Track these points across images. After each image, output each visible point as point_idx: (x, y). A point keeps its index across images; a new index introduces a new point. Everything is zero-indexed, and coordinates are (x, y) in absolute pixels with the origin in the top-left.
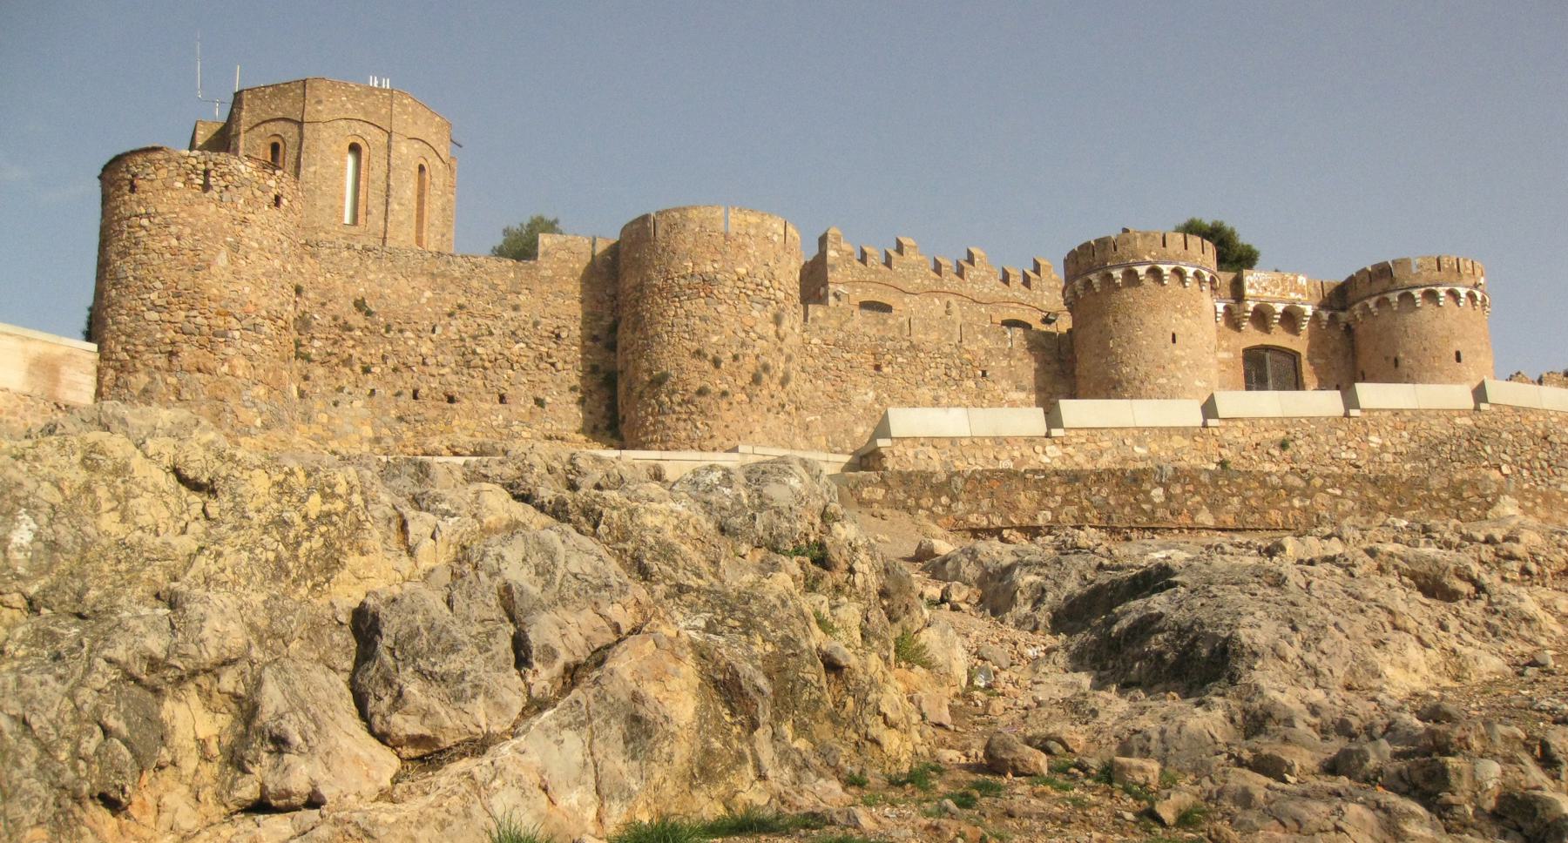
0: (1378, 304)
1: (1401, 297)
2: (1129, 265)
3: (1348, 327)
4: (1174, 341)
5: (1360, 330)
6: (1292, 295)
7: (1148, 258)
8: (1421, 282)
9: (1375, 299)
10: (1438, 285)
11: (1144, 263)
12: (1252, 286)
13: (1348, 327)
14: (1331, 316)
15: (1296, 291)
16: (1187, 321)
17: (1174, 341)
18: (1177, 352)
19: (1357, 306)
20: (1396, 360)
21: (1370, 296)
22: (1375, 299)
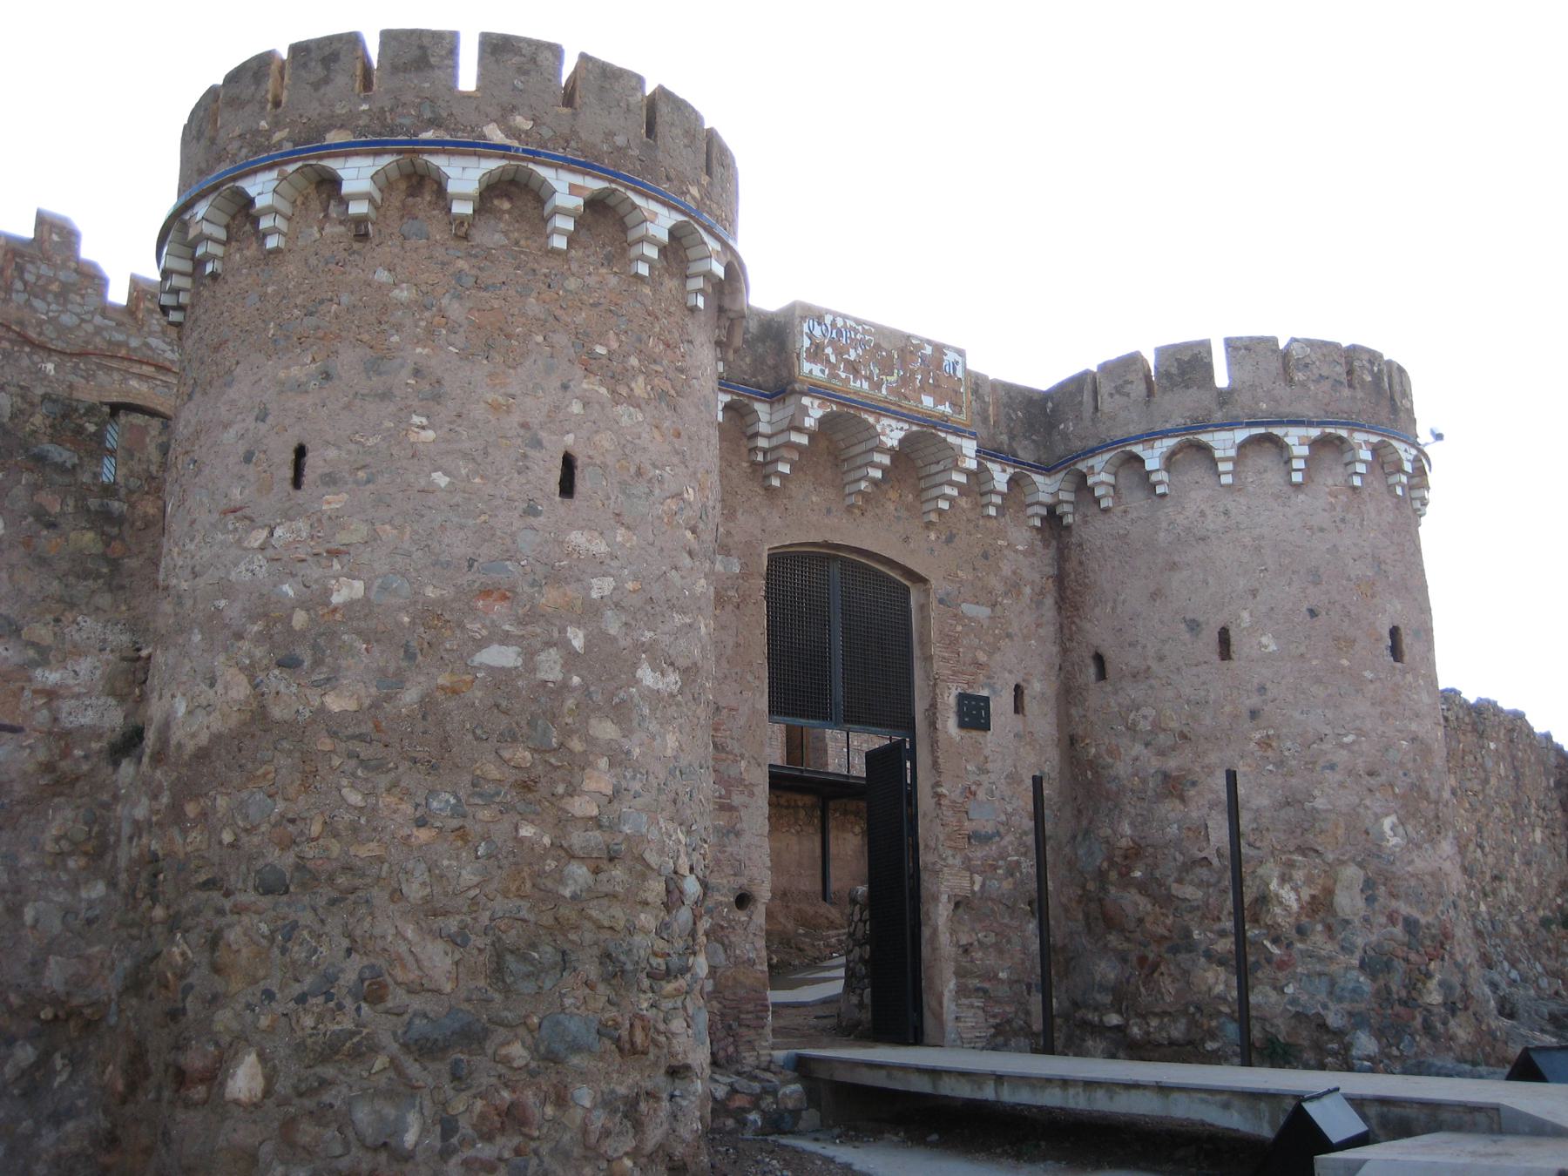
0: (1170, 460)
1: (1242, 446)
2: (414, 147)
3: (1052, 518)
4: (567, 487)
5: (1094, 533)
6: (928, 401)
7: (495, 134)
8: (1306, 409)
9: (1170, 443)
10: (1354, 426)
11: (477, 147)
12: (816, 353)
13: (1052, 518)
14: (1013, 482)
15: (935, 390)
16: (627, 416)
17: (567, 487)
18: (577, 538)
19: (1098, 462)
20: (1224, 639)
21: (1149, 437)
22: (1170, 443)
